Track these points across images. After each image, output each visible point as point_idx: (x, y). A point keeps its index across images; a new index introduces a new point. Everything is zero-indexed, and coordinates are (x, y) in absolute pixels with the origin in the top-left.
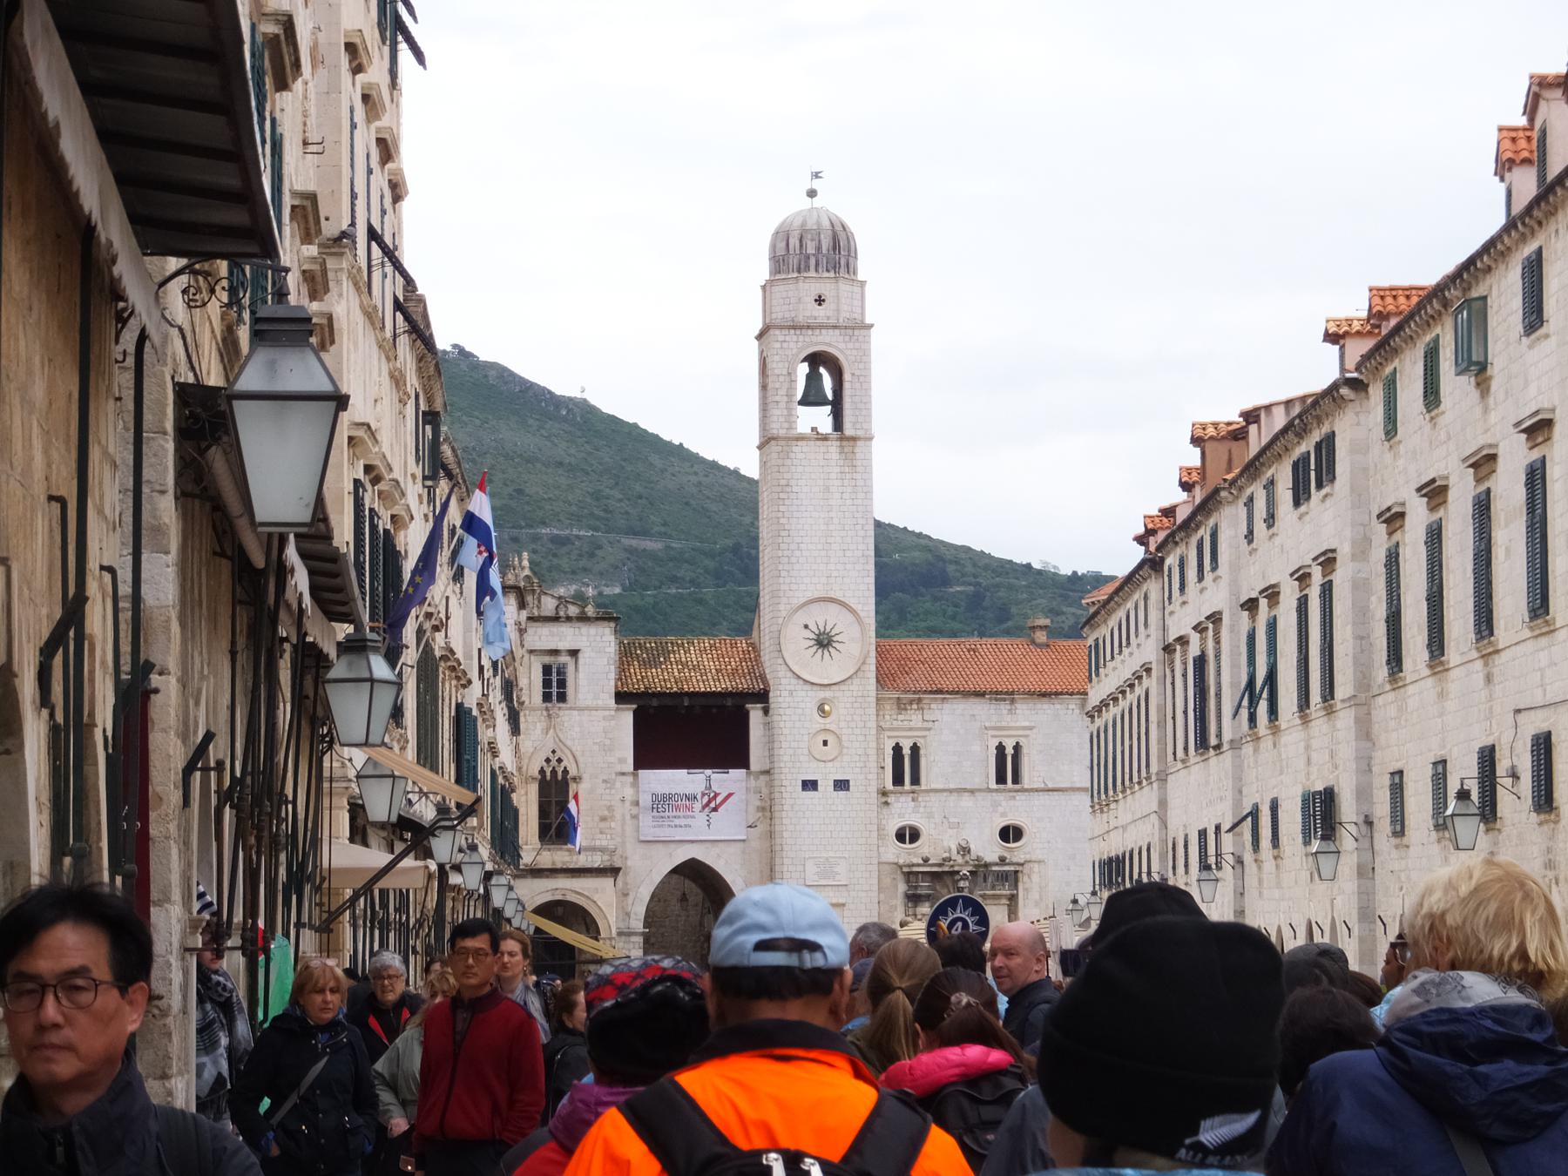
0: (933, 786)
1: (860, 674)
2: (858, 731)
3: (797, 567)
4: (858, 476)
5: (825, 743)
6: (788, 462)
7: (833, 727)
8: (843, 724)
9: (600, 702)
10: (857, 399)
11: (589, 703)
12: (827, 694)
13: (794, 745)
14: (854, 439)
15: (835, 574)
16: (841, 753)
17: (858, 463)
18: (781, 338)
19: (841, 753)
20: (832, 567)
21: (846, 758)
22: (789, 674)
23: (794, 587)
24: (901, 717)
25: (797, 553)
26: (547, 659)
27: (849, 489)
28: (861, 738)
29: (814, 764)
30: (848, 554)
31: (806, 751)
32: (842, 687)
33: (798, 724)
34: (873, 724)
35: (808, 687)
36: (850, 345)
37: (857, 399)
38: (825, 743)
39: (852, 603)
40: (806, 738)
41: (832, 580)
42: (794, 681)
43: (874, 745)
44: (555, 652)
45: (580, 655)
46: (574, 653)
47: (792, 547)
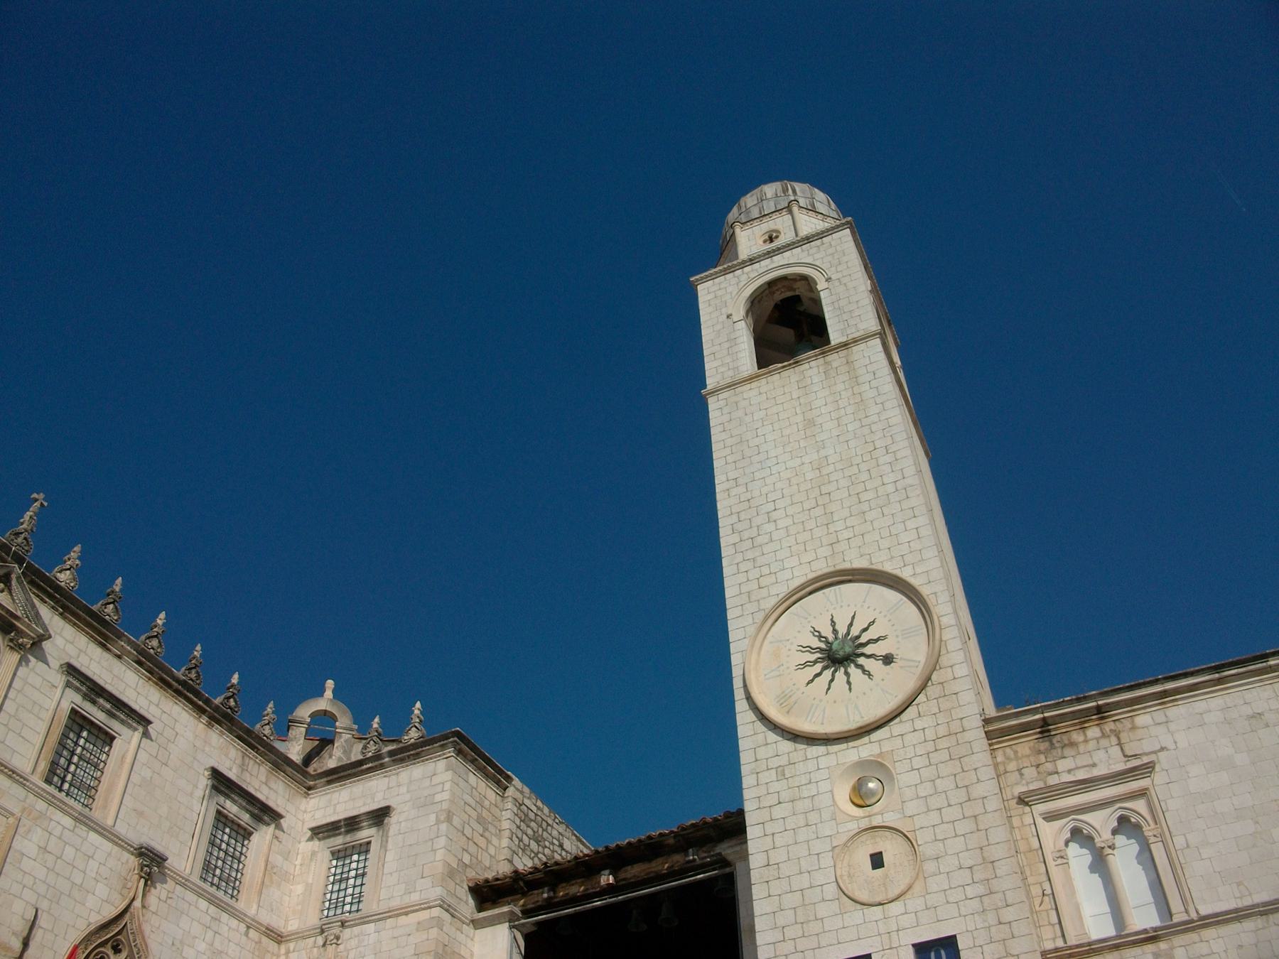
0: (1204, 911)
1: (931, 690)
2: (954, 813)
3: (766, 549)
4: (866, 387)
5: (877, 861)
6: (740, 413)
7: (890, 819)
8: (911, 808)
9: (415, 897)
10: (842, 303)
11: (396, 903)
12: (864, 749)
13: (804, 881)
14: (845, 345)
15: (846, 534)
16: (919, 874)
17: (862, 371)
18: (716, 288)
19: (919, 874)
20: (839, 526)
21: (935, 884)
22: (772, 737)
23: (764, 582)
24: (1062, 765)
25: (769, 527)
26: (338, 841)
27: (850, 410)
28: (963, 827)
29: (857, 915)
30: (864, 497)
31: (831, 890)
32: (896, 727)
33: (803, 835)
34: (987, 787)
35: (821, 749)
36: (817, 256)
37: (842, 303)
38: (877, 861)
39: (888, 568)
40: (827, 861)
41: (843, 546)
42: (786, 746)
43: (999, 834)
44: (352, 824)
45: (393, 821)
46: (380, 816)
47: (758, 521)
